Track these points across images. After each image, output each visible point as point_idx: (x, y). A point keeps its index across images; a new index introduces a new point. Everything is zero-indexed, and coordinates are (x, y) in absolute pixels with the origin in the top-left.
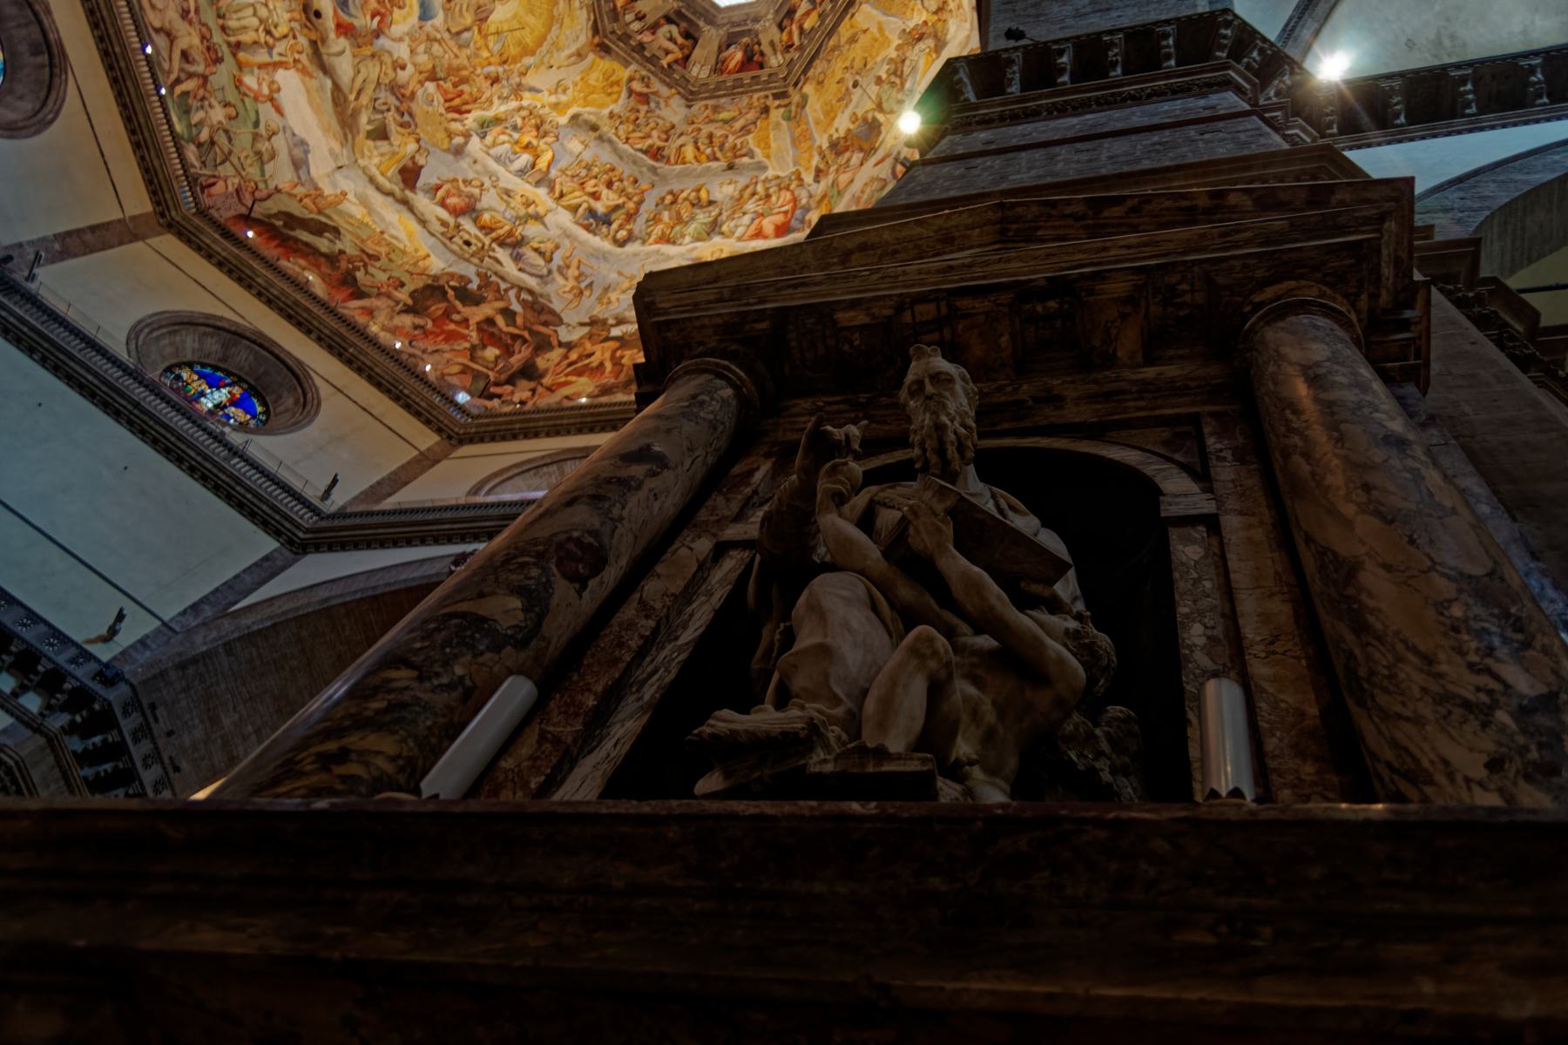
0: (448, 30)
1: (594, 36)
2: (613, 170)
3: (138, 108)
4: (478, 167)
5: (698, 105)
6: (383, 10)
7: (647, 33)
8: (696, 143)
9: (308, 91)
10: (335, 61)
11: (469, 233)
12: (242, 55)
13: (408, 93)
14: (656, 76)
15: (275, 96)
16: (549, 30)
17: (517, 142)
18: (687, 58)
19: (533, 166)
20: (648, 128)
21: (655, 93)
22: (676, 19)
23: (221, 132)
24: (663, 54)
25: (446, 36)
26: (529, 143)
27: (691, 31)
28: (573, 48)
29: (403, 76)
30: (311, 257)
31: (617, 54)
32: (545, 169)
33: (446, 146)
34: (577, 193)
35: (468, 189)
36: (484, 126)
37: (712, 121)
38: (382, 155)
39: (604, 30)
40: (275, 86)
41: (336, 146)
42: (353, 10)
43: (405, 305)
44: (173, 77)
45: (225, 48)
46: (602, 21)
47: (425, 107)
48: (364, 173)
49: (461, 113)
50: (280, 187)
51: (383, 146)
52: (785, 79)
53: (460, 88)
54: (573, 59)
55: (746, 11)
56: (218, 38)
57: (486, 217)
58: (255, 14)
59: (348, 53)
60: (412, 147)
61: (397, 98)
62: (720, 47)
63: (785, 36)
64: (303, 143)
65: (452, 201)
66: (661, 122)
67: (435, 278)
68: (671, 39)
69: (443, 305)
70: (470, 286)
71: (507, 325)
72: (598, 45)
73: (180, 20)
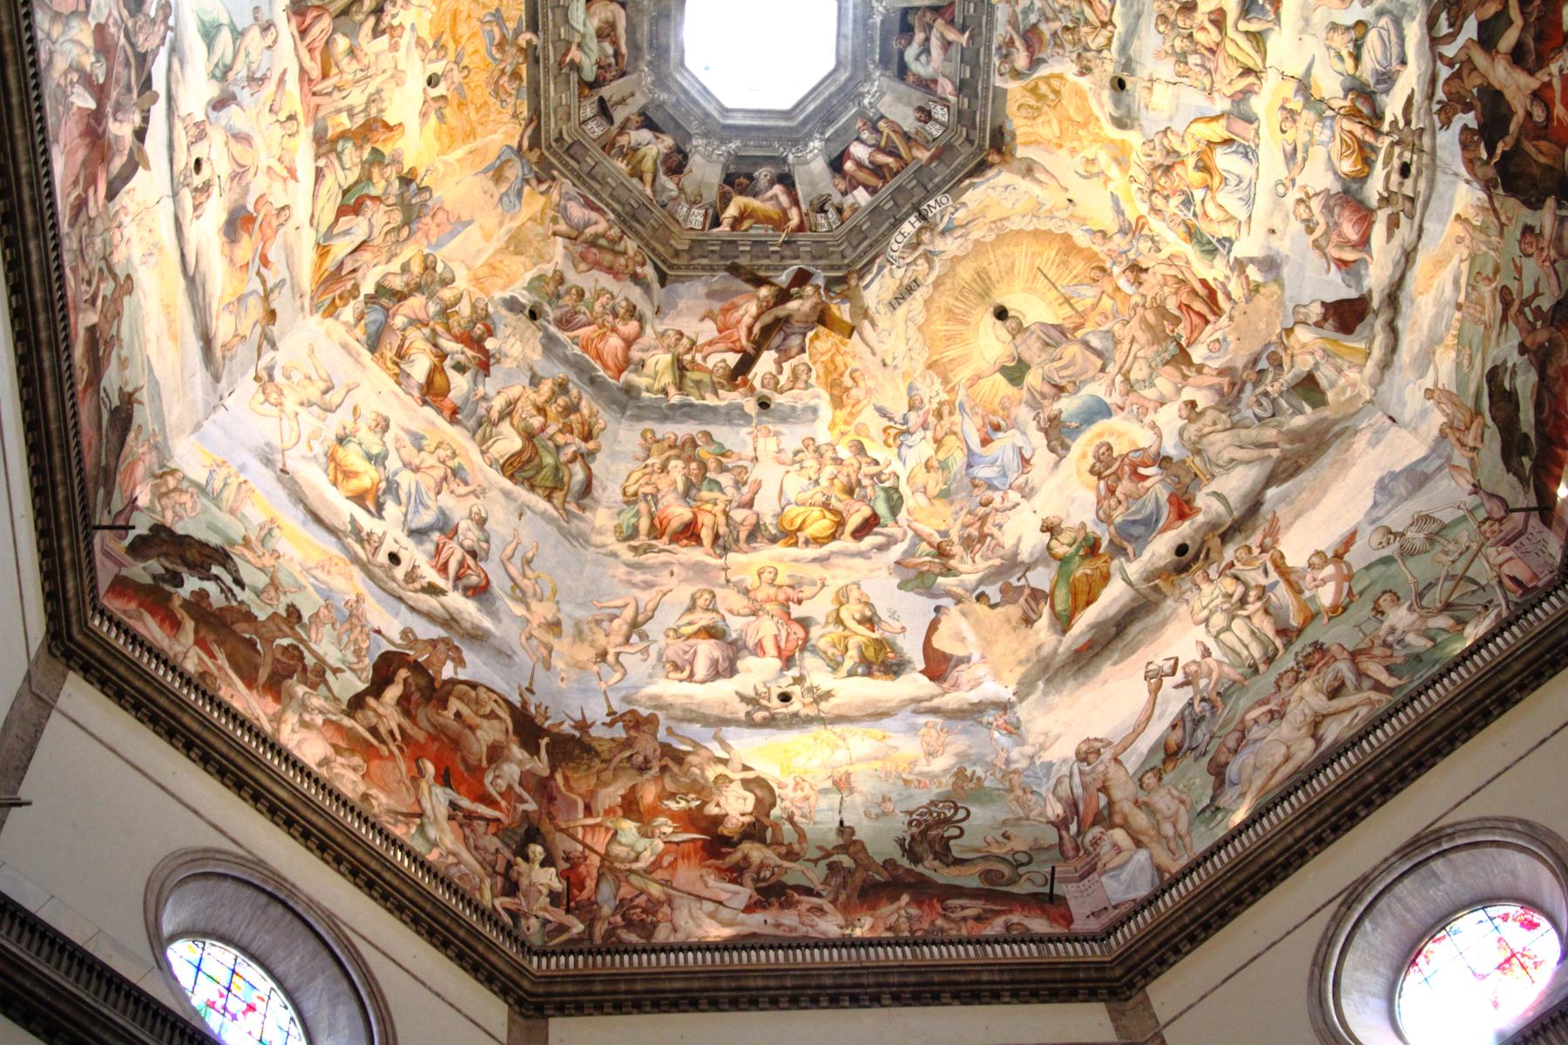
0: (1103, 369)
1: (991, 166)
2: (1163, 17)
3: (1443, 722)
4: (1277, 223)
6: (1127, 469)
7: (939, 91)
9: (1299, 515)
10: (1234, 499)
11: (1388, 177)
12: (1295, 622)
13: (1225, 381)
14: (990, 41)
15: (1330, 555)
16: (1019, 232)
17: (1208, 187)
19: (1227, 142)
21: (1013, 23)
22: (895, 60)
23: (1425, 602)
25: (1112, 369)
26: (1197, 168)
27: (897, 27)
28: (1024, 184)
29: (1203, 399)
30: (1556, 389)
32: (1223, 122)
33: (1274, 288)
34: (1231, 49)
35: (1319, 218)
36: (1210, 249)
38: (1340, 371)
39: (975, 155)
40: (1316, 560)
41: (1361, 442)
42: (1150, 507)
43: (1560, 206)
44: (1374, 695)
45: (1297, 647)
46: (964, 166)
47: (1232, 346)
48: (1381, 381)
49: (1212, 294)
50: (1470, 488)
51: (1324, 376)
53: (1177, 313)
54: (1040, 176)
56: (1287, 662)
57: (1347, 166)
58: (1228, 628)
59: (1213, 487)
60: (1303, 335)
61: (1241, 391)
64: (1382, 487)
65: (1351, 232)
67: (1488, 186)
68: (926, 49)
69: (1528, 146)
70: (1474, 125)
71: (1511, 23)
72: (1000, 152)
73: (1289, 716)
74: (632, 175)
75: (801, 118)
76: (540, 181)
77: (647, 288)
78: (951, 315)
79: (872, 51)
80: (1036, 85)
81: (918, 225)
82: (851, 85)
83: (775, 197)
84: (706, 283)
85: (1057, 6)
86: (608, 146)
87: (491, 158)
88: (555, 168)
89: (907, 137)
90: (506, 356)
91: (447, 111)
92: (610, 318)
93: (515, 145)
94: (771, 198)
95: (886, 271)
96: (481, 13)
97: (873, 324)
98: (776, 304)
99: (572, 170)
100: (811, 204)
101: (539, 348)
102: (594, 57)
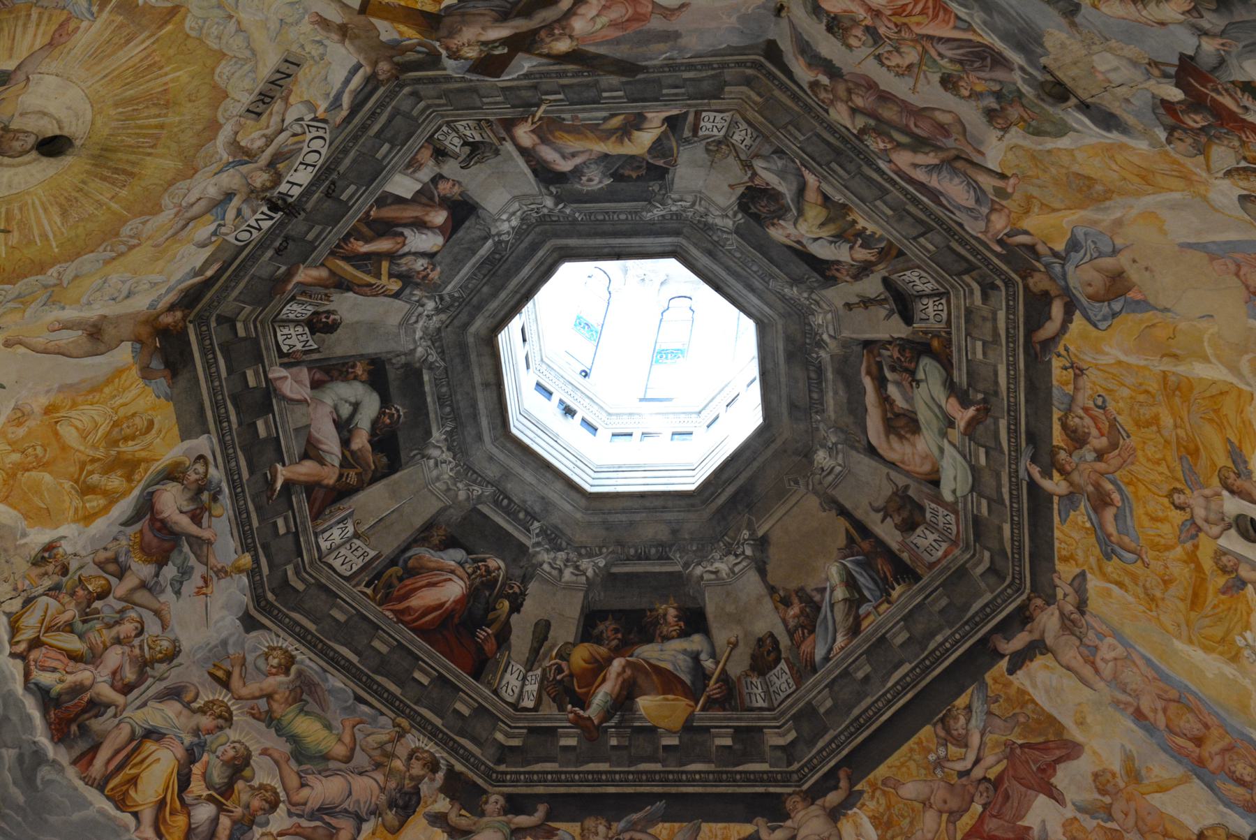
1: (172, 308)
5: (261, 640)
7: (304, 374)
8: (192, 756)
14: (235, 497)
18: (341, 492)
20: (108, 635)
21: (200, 546)
24: (297, 451)
31: (198, 380)
37: (270, 719)
46: (226, 288)
52: (504, 753)
55: (554, 493)
62: (429, 526)
63: (581, 655)
66: (153, 627)
68: (344, 427)
72: (163, 333)
74: (844, 206)
75: (540, 253)
76: (1031, 248)
77: (805, 48)
78: (165, 101)
79: (436, 383)
80: (129, 478)
81: (284, 188)
82: (463, 317)
83: (564, 157)
84: (682, 50)
85: (133, 614)
86: (890, 253)
87: (1130, 322)
88: (997, 255)
89: (343, 285)
90: (1134, 63)
91: (1222, 460)
92: (882, 30)
93: (1078, 321)
94: (574, 155)
95: (322, 106)
96: (1138, 568)
97: (323, 23)
98: (535, 32)
99: (963, 242)
100: (497, 152)
101: (1049, 43)
102: (921, 393)
